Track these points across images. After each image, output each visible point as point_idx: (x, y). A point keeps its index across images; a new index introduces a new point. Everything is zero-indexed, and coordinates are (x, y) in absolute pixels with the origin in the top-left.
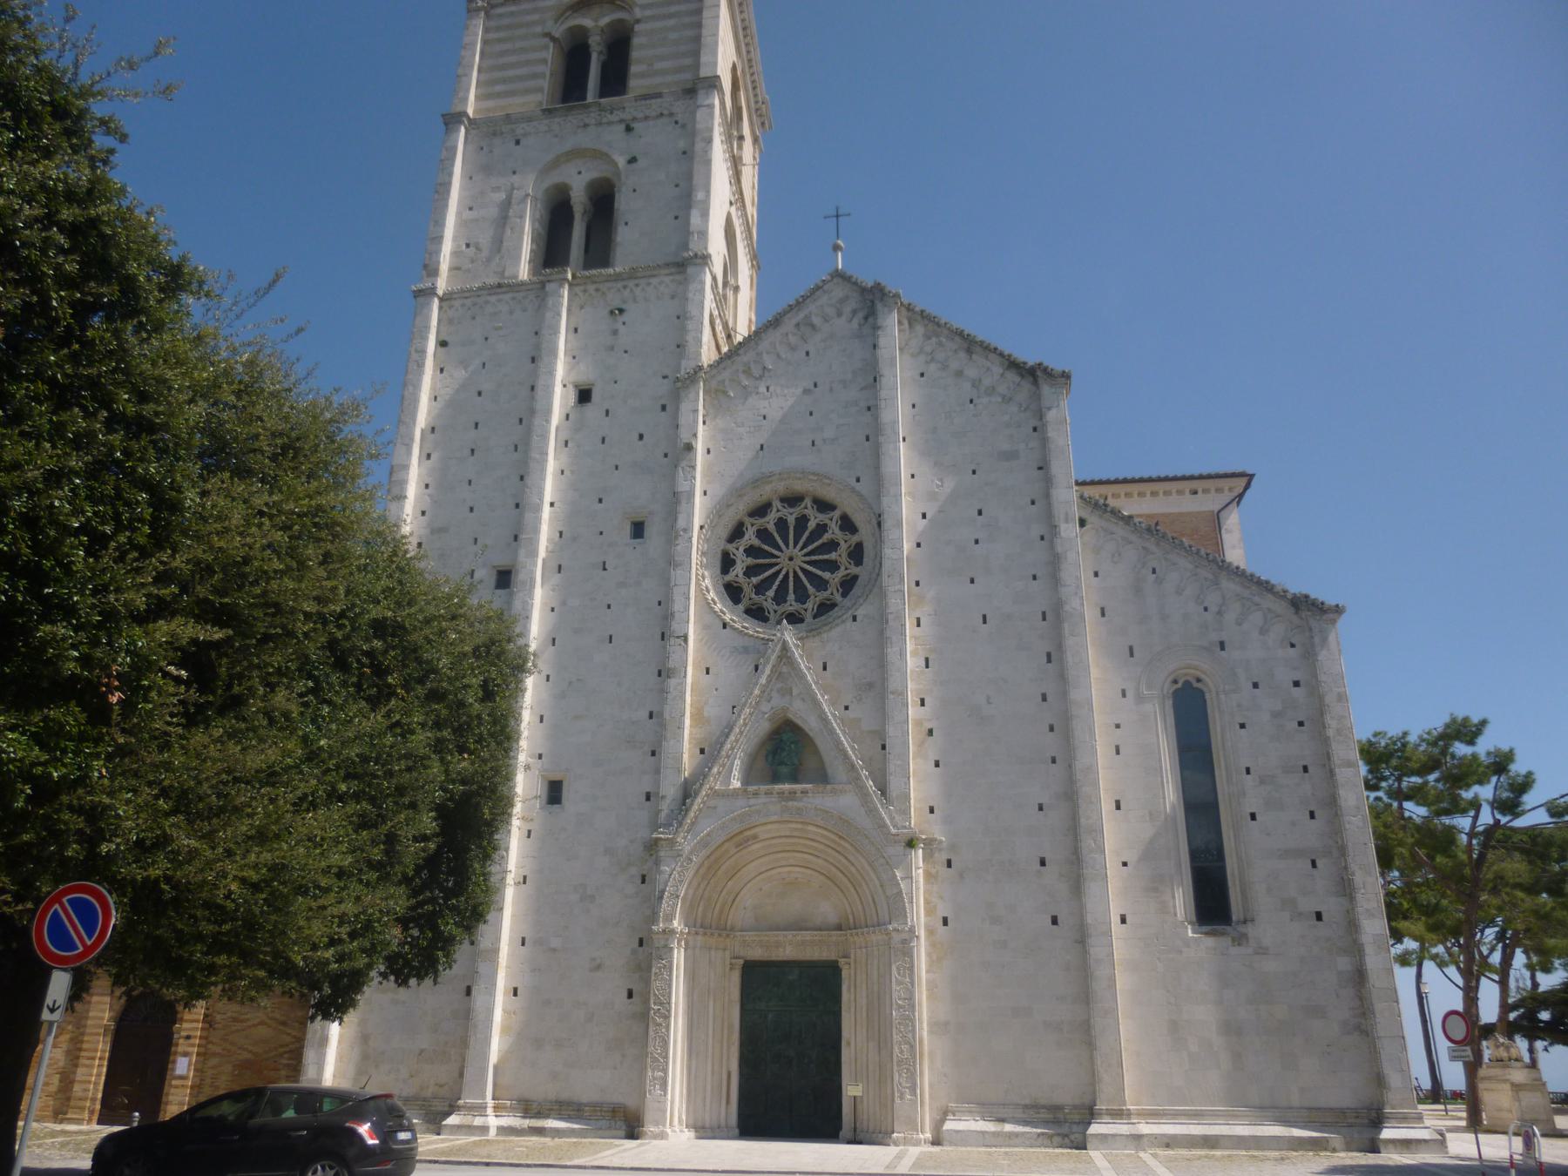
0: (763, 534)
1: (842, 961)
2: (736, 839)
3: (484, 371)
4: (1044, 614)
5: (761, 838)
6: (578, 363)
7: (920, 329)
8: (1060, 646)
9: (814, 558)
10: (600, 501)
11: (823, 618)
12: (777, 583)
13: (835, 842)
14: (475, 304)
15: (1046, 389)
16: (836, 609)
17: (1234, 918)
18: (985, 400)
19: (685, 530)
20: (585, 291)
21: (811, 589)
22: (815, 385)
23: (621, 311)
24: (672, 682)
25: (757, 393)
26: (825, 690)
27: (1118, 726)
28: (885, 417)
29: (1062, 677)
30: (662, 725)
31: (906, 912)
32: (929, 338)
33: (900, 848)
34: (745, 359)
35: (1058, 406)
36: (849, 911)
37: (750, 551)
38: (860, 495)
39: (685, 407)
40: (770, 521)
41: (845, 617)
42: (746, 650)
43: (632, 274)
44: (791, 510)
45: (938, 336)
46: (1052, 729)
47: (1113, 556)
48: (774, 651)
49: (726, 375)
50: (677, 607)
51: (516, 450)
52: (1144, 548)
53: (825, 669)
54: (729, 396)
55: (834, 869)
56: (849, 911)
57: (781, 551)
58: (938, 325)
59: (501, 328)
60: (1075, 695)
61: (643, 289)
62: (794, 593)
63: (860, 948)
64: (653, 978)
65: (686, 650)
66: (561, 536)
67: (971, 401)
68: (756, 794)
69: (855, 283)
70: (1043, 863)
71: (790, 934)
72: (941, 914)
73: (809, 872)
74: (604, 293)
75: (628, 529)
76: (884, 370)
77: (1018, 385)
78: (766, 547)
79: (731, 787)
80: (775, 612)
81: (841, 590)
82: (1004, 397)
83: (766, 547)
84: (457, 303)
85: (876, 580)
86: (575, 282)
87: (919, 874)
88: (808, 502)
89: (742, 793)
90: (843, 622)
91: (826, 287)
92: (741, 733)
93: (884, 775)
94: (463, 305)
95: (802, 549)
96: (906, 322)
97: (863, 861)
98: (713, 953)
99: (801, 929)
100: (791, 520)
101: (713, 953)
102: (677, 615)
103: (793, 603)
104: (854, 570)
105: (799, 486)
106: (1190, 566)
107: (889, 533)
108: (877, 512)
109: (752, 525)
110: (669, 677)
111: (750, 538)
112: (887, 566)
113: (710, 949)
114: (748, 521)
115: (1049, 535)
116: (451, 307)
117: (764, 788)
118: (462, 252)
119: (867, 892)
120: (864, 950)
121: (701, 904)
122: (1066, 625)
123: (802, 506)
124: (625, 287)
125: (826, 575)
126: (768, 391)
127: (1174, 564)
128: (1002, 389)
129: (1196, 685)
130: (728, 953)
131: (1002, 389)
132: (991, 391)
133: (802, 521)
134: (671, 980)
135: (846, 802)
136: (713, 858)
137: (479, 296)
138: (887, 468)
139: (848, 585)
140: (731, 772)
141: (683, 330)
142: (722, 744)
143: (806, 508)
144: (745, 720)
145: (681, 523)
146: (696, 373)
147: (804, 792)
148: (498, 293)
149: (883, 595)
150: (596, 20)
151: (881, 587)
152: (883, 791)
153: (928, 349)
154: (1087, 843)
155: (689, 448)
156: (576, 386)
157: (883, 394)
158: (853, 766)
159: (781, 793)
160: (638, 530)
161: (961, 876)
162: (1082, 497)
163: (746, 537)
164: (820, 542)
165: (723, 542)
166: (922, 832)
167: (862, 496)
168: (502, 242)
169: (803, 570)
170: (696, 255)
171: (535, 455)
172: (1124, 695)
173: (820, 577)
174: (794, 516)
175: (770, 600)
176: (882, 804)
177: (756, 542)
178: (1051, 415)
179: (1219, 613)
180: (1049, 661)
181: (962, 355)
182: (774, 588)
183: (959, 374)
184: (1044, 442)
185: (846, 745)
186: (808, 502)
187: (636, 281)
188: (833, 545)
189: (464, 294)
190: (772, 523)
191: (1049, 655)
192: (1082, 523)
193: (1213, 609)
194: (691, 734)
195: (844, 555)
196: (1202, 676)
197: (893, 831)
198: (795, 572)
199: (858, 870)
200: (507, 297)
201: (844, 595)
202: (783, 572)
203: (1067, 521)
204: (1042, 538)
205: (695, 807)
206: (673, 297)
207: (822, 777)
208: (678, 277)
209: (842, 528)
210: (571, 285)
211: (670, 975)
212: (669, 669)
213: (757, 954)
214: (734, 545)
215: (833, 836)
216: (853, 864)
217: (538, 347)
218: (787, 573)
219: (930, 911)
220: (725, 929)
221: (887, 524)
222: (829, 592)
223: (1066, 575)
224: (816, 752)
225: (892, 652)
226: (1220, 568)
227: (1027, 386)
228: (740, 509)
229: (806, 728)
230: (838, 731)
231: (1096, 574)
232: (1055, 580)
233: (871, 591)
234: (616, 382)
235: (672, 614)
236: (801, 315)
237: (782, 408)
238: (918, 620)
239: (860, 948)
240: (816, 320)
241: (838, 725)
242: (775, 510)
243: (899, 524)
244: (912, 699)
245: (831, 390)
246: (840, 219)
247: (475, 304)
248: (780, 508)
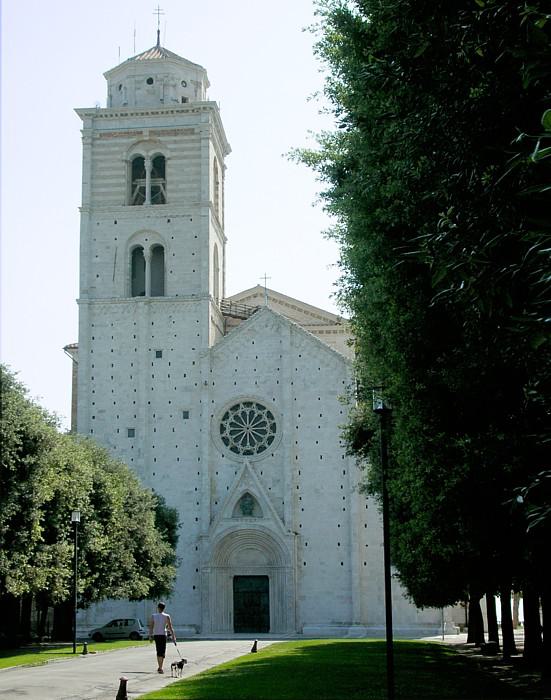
0: (236, 417)
111: (231, 419)
133: (252, 413)
150: (148, 151)
152: (284, 522)
160: (186, 415)
188: (264, 423)
227: (341, 364)
228: (227, 408)
240: (257, 329)
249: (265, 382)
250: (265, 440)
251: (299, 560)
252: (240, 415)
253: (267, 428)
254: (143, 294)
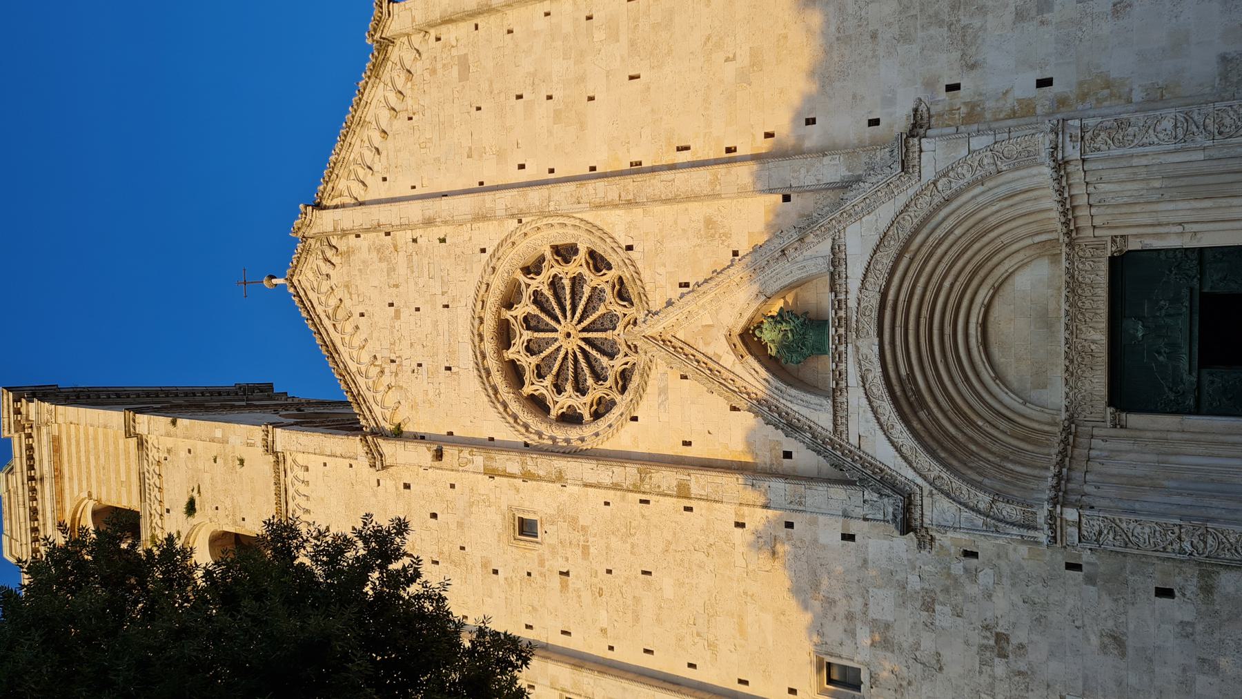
9: (568, 307)
10: (495, 572)
22: (391, 305)
67: (410, 119)
80: (626, 355)
88: (507, 314)
161: (973, 67)
169: (580, 322)
175: (612, 363)
188: (555, 284)
245: (396, 286)
250: (572, 269)
251: (1025, 110)
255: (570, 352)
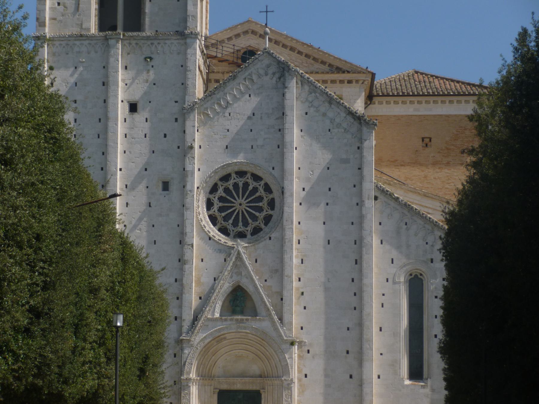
0: (226, 190)
1: (262, 391)
2: (217, 339)
3: (76, 88)
4: (355, 241)
5: (227, 338)
6: (128, 88)
7: (306, 87)
8: (361, 257)
11: (256, 236)
12: (234, 216)
13: (260, 341)
14: (67, 45)
15: (365, 129)
16: (262, 232)
17: (424, 377)
18: (336, 130)
19: (190, 191)
20: (130, 44)
21: (250, 221)
23: (151, 58)
24: (187, 267)
25: (224, 116)
26: (257, 273)
27: (383, 295)
28: (287, 138)
29: (361, 271)
30: (182, 285)
31: (289, 373)
32: (311, 93)
33: (288, 345)
34: (218, 96)
35: (370, 139)
36: (265, 370)
37: (221, 199)
38: (274, 177)
39: (188, 124)
40: (230, 184)
41: (266, 238)
42: (220, 251)
43: (156, 37)
44: (241, 179)
45: (315, 92)
46: (355, 294)
47: (389, 215)
48: (234, 255)
49: (208, 104)
50: (188, 230)
51: (99, 137)
52: (402, 213)
53: (256, 261)
54: (210, 117)
55: (259, 352)
56: (265, 370)
57: (236, 200)
58: (316, 87)
59: (83, 62)
60: (365, 281)
61: (162, 46)
62: (242, 221)
63: (270, 386)
64: (182, 398)
65: (193, 252)
66: (126, 187)
67: (329, 130)
68: (226, 320)
69: (275, 58)
70: (348, 352)
71: (239, 379)
72: (304, 373)
73: (248, 352)
74: (140, 46)
75: (161, 185)
76: (288, 112)
77: (353, 123)
78: (228, 198)
79: (215, 317)
80: (233, 231)
81: (264, 222)
82: (345, 129)
83: (228, 198)
84: (57, 43)
85: (280, 220)
86: (125, 38)
87: (296, 356)
88: (249, 175)
89: (220, 319)
90: (265, 240)
91: (260, 58)
92: (219, 292)
93: (282, 312)
94: (60, 45)
95: (246, 200)
96: (300, 83)
97: (272, 350)
98: (206, 387)
99: (244, 377)
100: (241, 185)
101: (206, 387)
102: (188, 234)
103: (242, 227)
104: (270, 212)
105: (244, 169)
106: (422, 223)
107: (287, 200)
108: (282, 186)
109: (222, 186)
110: (185, 264)
111: (220, 192)
112: (285, 215)
113: (205, 385)
114: (220, 183)
115: (360, 204)
116: (53, 45)
117: (229, 318)
118: (55, 8)
119: (273, 363)
120: (271, 387)
121: (202, 366)
122: (364, 249)
123: (246, 178)
124: (152, 44)
125: (257, 214)
126: (230, 115)
127: (416, 221)
128: (345, 125)
129: (420, 276)
130: (212, 387)
131: (345, 125)
132: (339, 126)
133: (246, 185)
134: (190, 399)
135: (265, 325)
136: (206, 347)
137: (69, 40)
138: (287, 165)
139: (268, 219)
140: (215, 310)
141: (185, 78)
142: (211, 297)
143: (248, 178)
144: (221, 286)
145: (188, 187)
146: (194, 105)
147: (247, 320)
148: (80, 40)
149: (283, 229)
151: (283, 224)
152: (281, 319)
153: (310, 99)
154: (366, 346)
155: (191, 147)
156: (128, 102)
157: (287, 126)
158: (268, 309)
159: (237, 320)
160: (166, 186)
161: (313, 357)
162: (377, 186)
163: (219, 192)
164: (254, 197)
165: (208, 194)
166: (297, 338)
167: (275, 177)
168: (79, 4)
169: (245, 210)
170: (192, 32)
171: (110, 143)
172: (387, 281)
173: (254, 214)
174: (242, 182)
175: (230, 225)
176: (281, 326)
177: (224, 195)
178: (366, 144)
179: (432, 246)
180: (356, 263)
181: (327, 104)
182: (233, 218)
183: (324, 115)
184: (362, 157)
185: (266, 300)
186: (249, 175)
187: (158, 41)
189: (61, 38)
190: (231, 185)
191: (356, 260)
192: (376, 198)
193: (430, 243)
194: (195, 290)
195: (266, 204)
196: (423, 274)
197: (285, 338)
198: (242, 211)
199: (269, 353)
200: (87, 42)
201: (266, 224)
202: (237, 211)
203: (368, 199)
204: (357, 204)
205: (199, 325)
206: (179, 54)
207: (255, 313)
208: (182, 42)
209: (265, 190)
210: (122, 39)
211: (190, 397)
212: (185, 260)
213: (225, 387)
214: (213, 195)
215: (259, 339)
216: (267, 351)
217: (107, 76)
218: (239, 211)
219: (300, 371)
220: (211, 377)
221: (287, 194)
222: (258, 222)
223: (366, 225)
224: (252, 300)
225: (286, 257)
226: (435, 225)
227: (356, 124)
229: (248, 290)
230: (262, 294)
231: (380, 224)
232: (361, 227)
233: (278, 226)
234: (150, 102)
235: (186, 233)
236: (247, 74)
237: (237, 126)
238: (299, 241)
239: (270, 386)
240: (255, 77)
241: (262, 290)
242: (233, 178)
243: (292, 195)
244: (295, 278)
245: (261, 118)
246: (268, 13)
247: (67, 45)
248: (236, 178)
249: (262, 146)
252: (231, 188)
253: (264, 204)
254: (114, 28)
255: (235, 205)
